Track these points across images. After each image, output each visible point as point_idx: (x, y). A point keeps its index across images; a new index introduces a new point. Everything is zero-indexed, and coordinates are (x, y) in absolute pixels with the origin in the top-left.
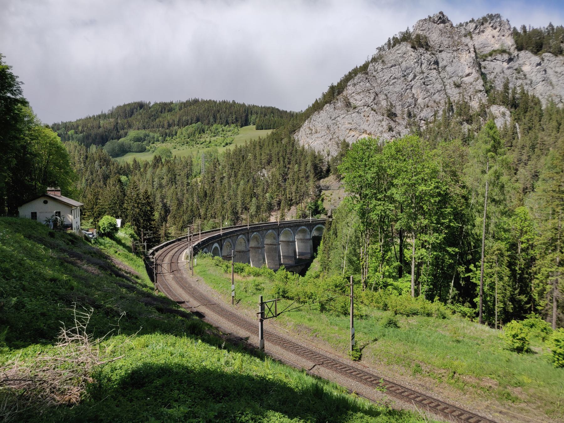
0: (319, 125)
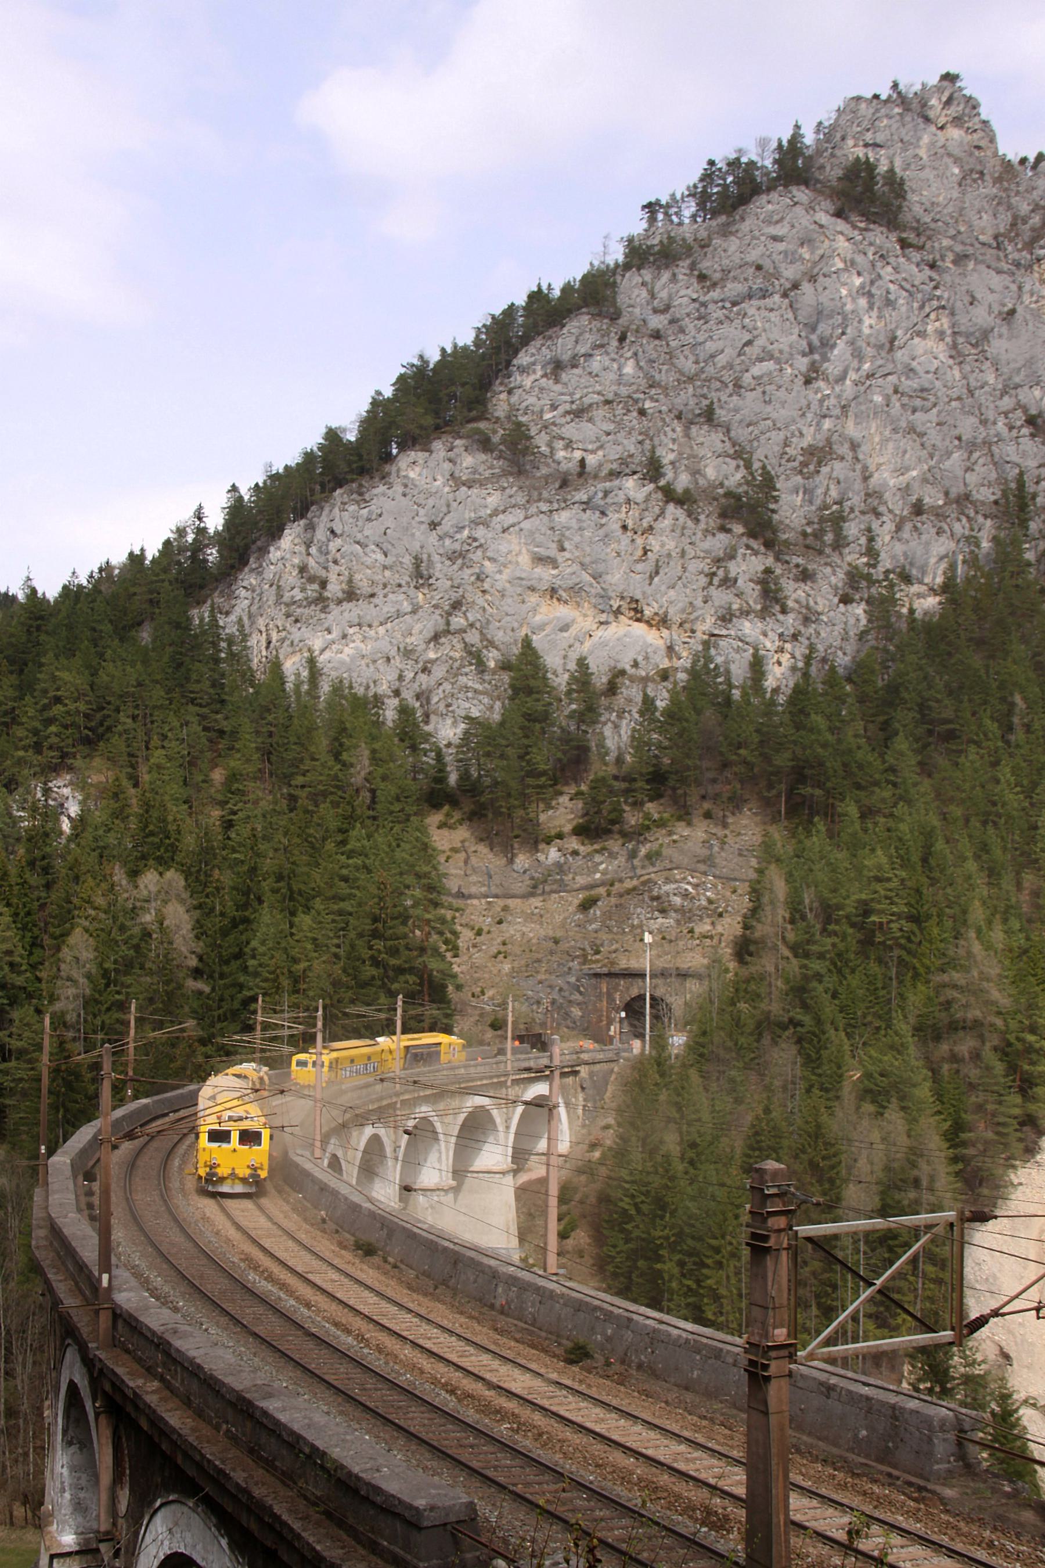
0: (368, 561)
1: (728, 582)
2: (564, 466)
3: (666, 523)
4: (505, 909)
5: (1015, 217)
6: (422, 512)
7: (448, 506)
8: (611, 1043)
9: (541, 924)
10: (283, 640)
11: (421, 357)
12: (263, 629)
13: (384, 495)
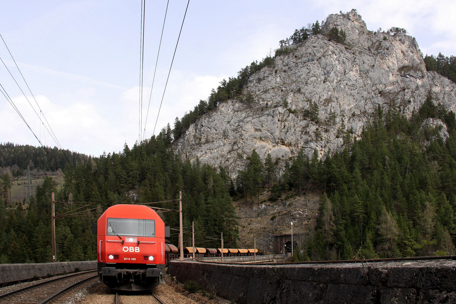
1: (307, 133)
2: (262, 106)
3: (290, 118)
5: (372, 43)
6: (225, 119)
7: (232, 117)
10: (190, 155)
11: (224, 80)
12: (185, 153)
13: (215, 115)
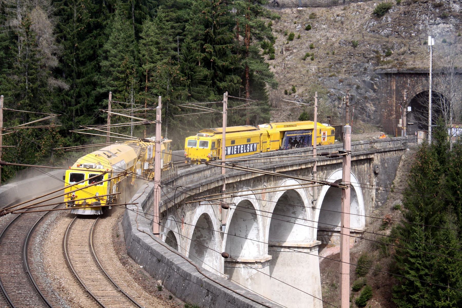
4: (313, 16)
8: (400, 134)
9: (342, 30)
